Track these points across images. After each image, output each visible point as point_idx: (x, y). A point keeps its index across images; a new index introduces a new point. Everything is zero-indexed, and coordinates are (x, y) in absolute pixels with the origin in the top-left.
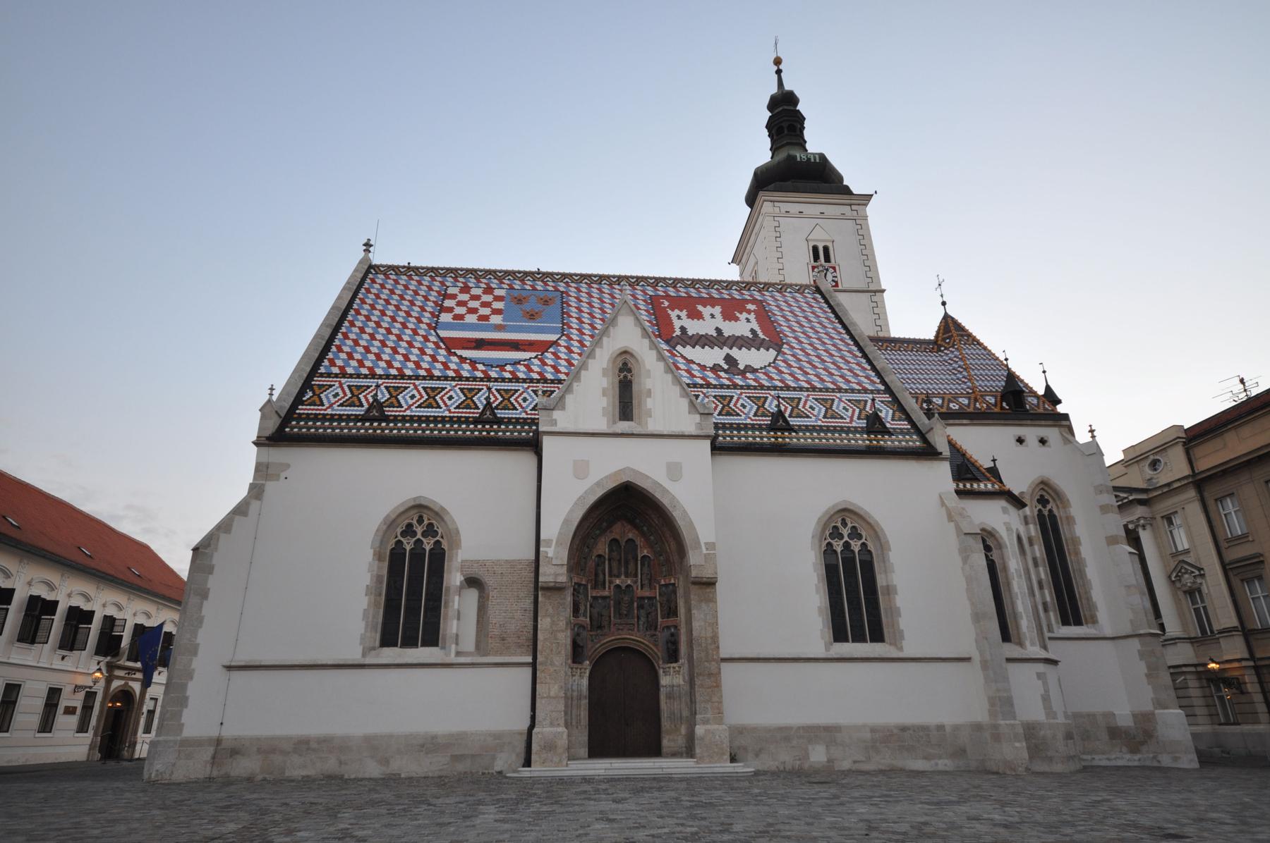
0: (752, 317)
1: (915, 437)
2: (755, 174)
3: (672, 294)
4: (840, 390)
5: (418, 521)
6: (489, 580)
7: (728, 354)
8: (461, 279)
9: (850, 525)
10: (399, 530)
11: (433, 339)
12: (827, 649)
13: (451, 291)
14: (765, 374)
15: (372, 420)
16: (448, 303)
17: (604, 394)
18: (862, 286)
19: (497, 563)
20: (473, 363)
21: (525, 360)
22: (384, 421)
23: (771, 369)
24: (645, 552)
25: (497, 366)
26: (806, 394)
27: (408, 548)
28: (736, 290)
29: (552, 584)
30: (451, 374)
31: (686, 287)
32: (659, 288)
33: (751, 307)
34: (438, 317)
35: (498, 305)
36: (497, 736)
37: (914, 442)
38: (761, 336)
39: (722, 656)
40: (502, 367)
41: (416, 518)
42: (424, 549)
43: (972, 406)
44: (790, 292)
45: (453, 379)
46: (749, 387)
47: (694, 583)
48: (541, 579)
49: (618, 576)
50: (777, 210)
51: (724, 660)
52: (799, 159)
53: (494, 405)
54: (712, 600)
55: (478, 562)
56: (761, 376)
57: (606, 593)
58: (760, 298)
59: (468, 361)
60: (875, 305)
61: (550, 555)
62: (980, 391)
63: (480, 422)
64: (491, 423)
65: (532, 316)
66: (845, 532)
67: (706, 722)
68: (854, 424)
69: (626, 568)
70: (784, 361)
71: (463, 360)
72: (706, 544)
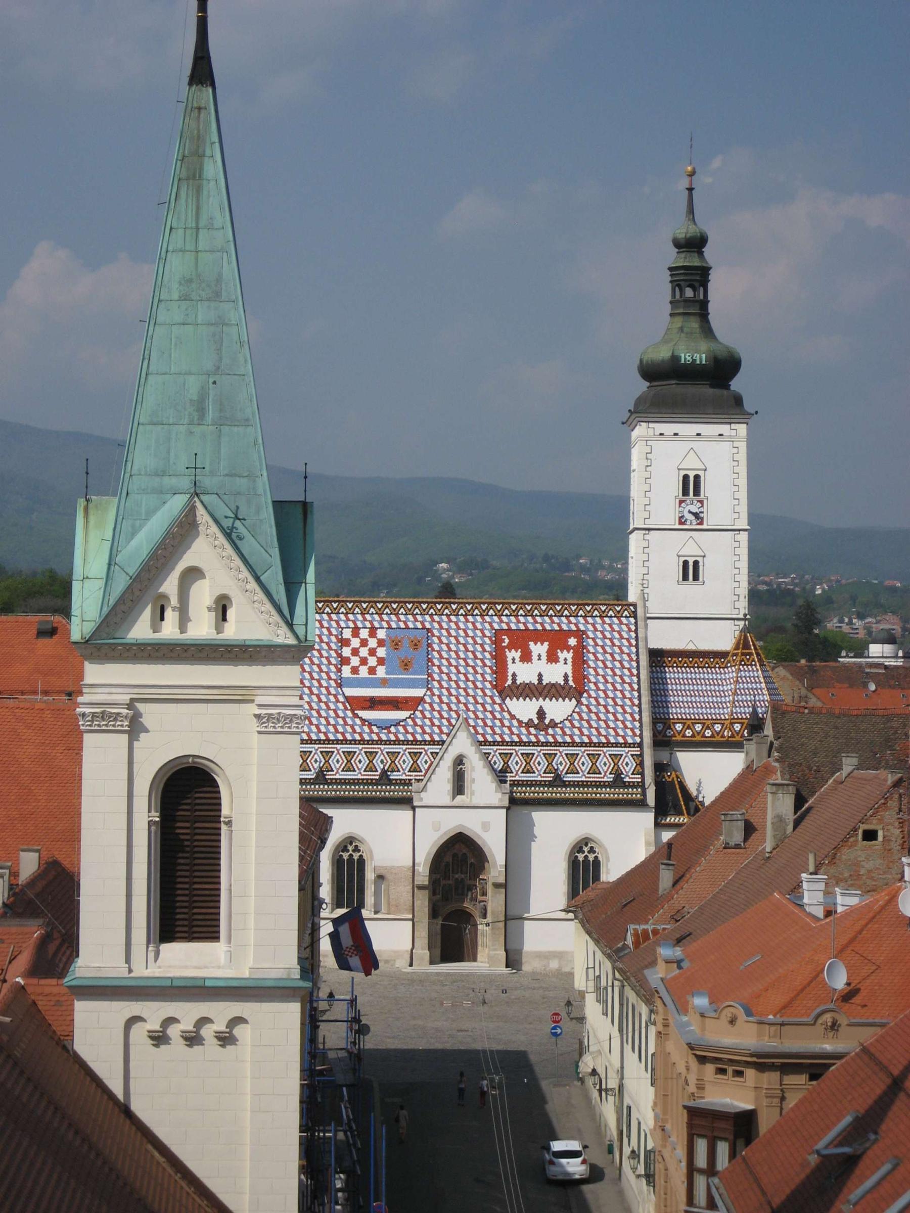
0: (569, 656)
1: (639, 790)
2: (641, 361)
3: (513, 627)
4: (608, 744)
6: (388, 876)
7: (541, 707)
8: (351, 617)
9: (589, 845)
10: (340, 849)
11: (341, 699)
13: (347, 634)
14: (562, 729)
15: (319, 784)
16: (346, 652)
17: (448, 782)
18: (726, 523)
19: (392, 867)
20: (370, 725)
22: (326, 784)
23: (567, 723)
24: (472, 860)
25: (387, 728)
26: (583, 749)
28: (566, 616)
30: (357, 737)
31: (526, 615)
32: (504, 619)
33: (572, 642)
34: (339, 670)
35: (381, 652)
36: (395, 952)
37: (636, 794)
38: (571, 683)
40: (388, 728)
43: (721, 733)
44: (611, 617)
45: (359, 744)
46: (547, 744)
48: (416, 883)
49: (457, 873)
50: (651, 432)
52: (683, 361)
53: (386, 768)
55: (382, 867)
56: (558, 731)
57: (450, 882)
58: (582, 628)
59: (367, 723)
60: (737, 544)
62: (734, 719)
63: (380, 785)
64: (386, 785)
65: (406, 666)
66: (586, 849)
68: (605, 779)
69: (461, 870)
70: (579, 713)
71: (363, 721)
72: (500, 865)
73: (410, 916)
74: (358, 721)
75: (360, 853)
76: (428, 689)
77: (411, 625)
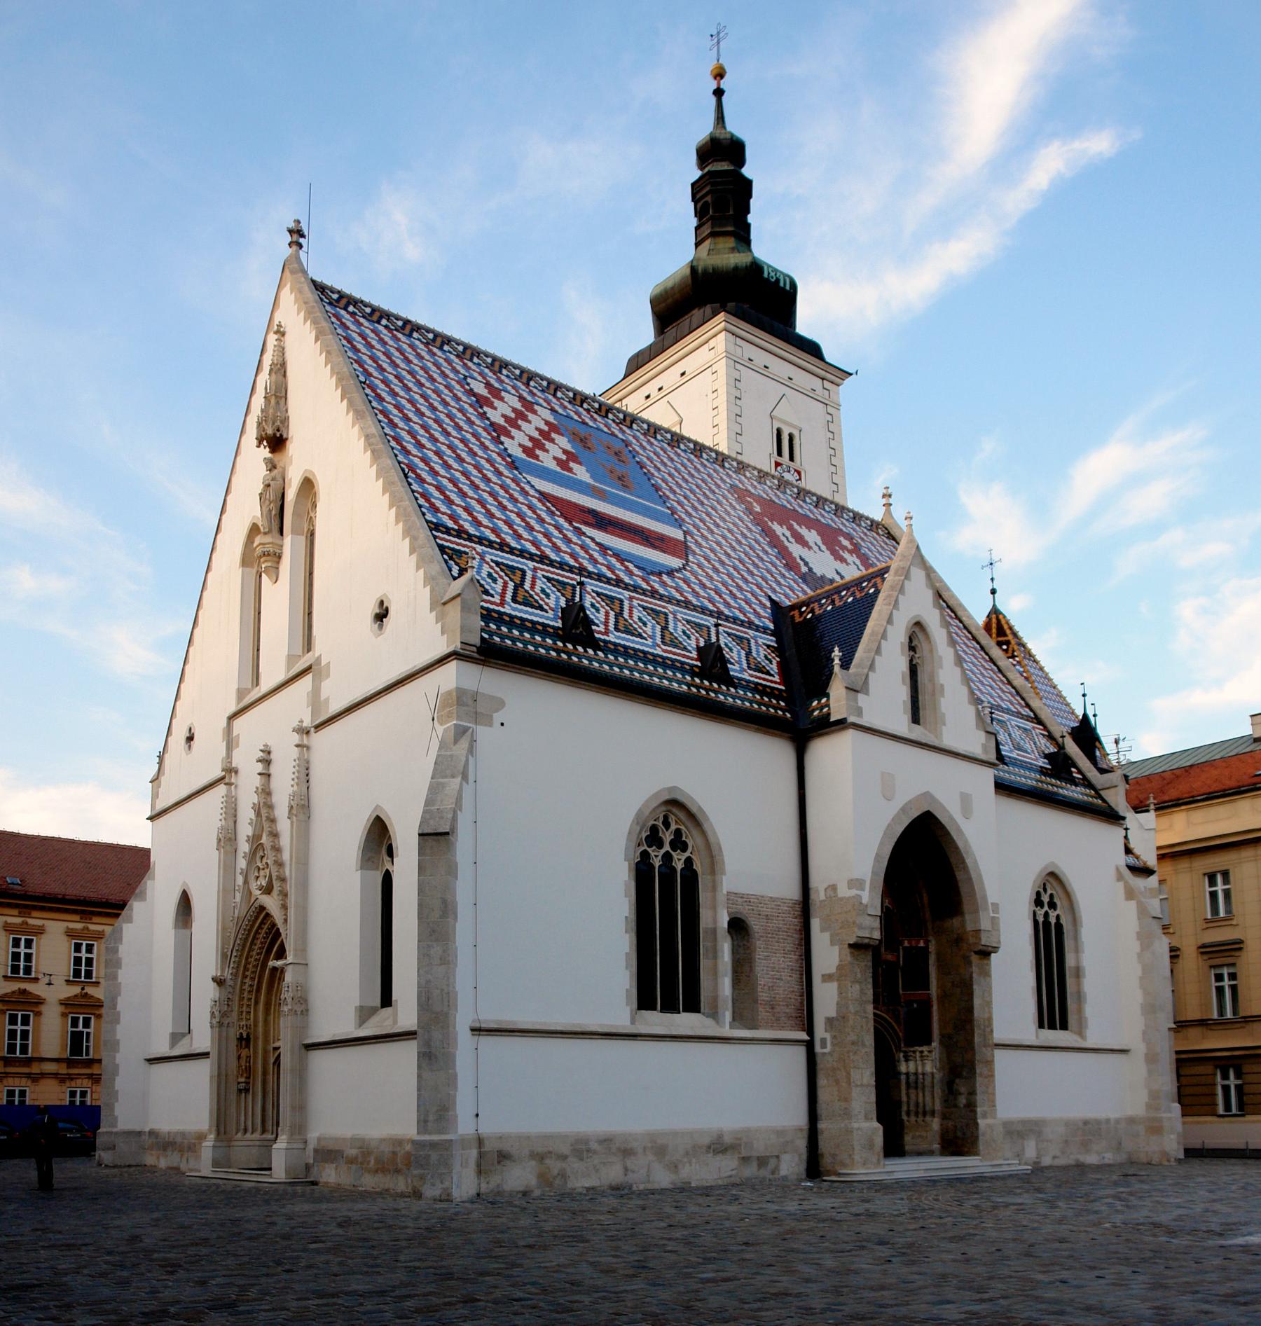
5: (663, 823)
6: (756, 925)
10: (644, 836)
11: (532, 492)
12: (1037, 1037)
17: (904, 682)
19: (761, 900)
20: (617, 555)
21: (677, 571)
25: (653, 573)
27: (657, 863)
29: (866, 941)
34: (502, 443)
39: (996, 1041)
41: (661, 819)
42: (674, 870)
47: (976, 953)
51: (999, 1046)
54: (986, 974)
61: (865, 900)
65: (622, 481)
67: (985, 1116)
71: (603, 548)
73: (807, 1038)
74: (588, 541)
75: (687, 854)
76: (686, 533)
77: (591, 424)
